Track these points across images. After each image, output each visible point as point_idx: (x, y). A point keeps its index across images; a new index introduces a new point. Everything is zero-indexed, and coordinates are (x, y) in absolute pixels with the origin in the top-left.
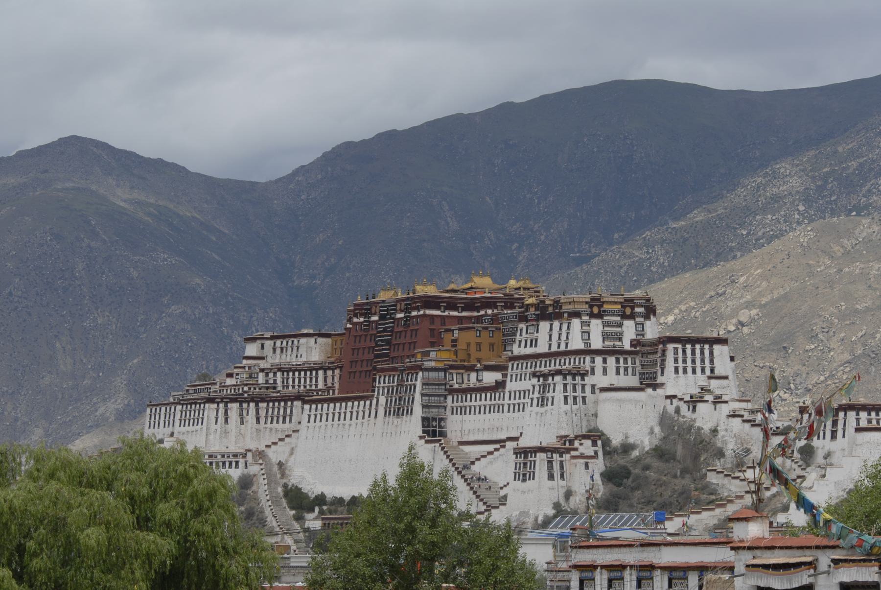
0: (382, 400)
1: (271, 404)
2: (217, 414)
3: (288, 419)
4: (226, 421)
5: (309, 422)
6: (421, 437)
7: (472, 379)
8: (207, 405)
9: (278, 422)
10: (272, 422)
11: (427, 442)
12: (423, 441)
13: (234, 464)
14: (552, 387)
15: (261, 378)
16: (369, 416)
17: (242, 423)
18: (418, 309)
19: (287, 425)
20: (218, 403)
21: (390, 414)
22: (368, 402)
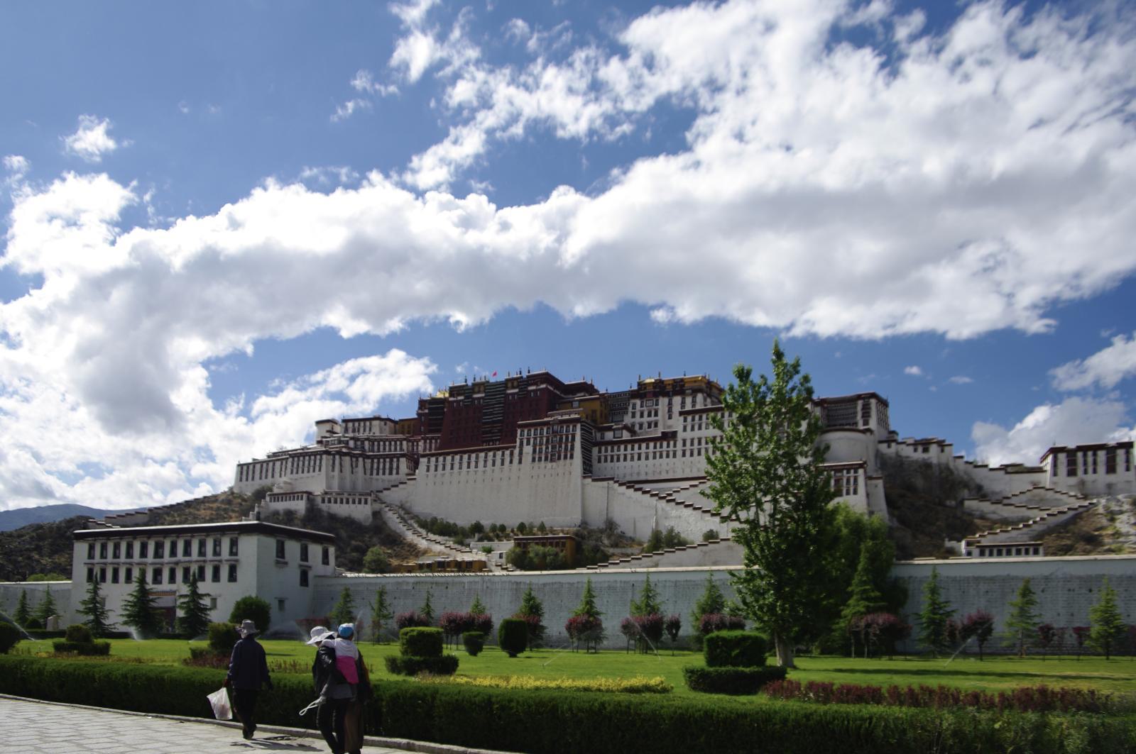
0: (528, 449)
2: (334, 463)
3: (394, 472)
5: (428, 470)
7: (609, 436)
8: (324, 456)
9: (384, 474)
10: (378, 474)
11: (594, 480)
15: (351, 444)
16: (511, 462)
17: (352, 473)
19: (394, 476)
20: (334, 455)
21: (540, 459)
22: (508, 452)
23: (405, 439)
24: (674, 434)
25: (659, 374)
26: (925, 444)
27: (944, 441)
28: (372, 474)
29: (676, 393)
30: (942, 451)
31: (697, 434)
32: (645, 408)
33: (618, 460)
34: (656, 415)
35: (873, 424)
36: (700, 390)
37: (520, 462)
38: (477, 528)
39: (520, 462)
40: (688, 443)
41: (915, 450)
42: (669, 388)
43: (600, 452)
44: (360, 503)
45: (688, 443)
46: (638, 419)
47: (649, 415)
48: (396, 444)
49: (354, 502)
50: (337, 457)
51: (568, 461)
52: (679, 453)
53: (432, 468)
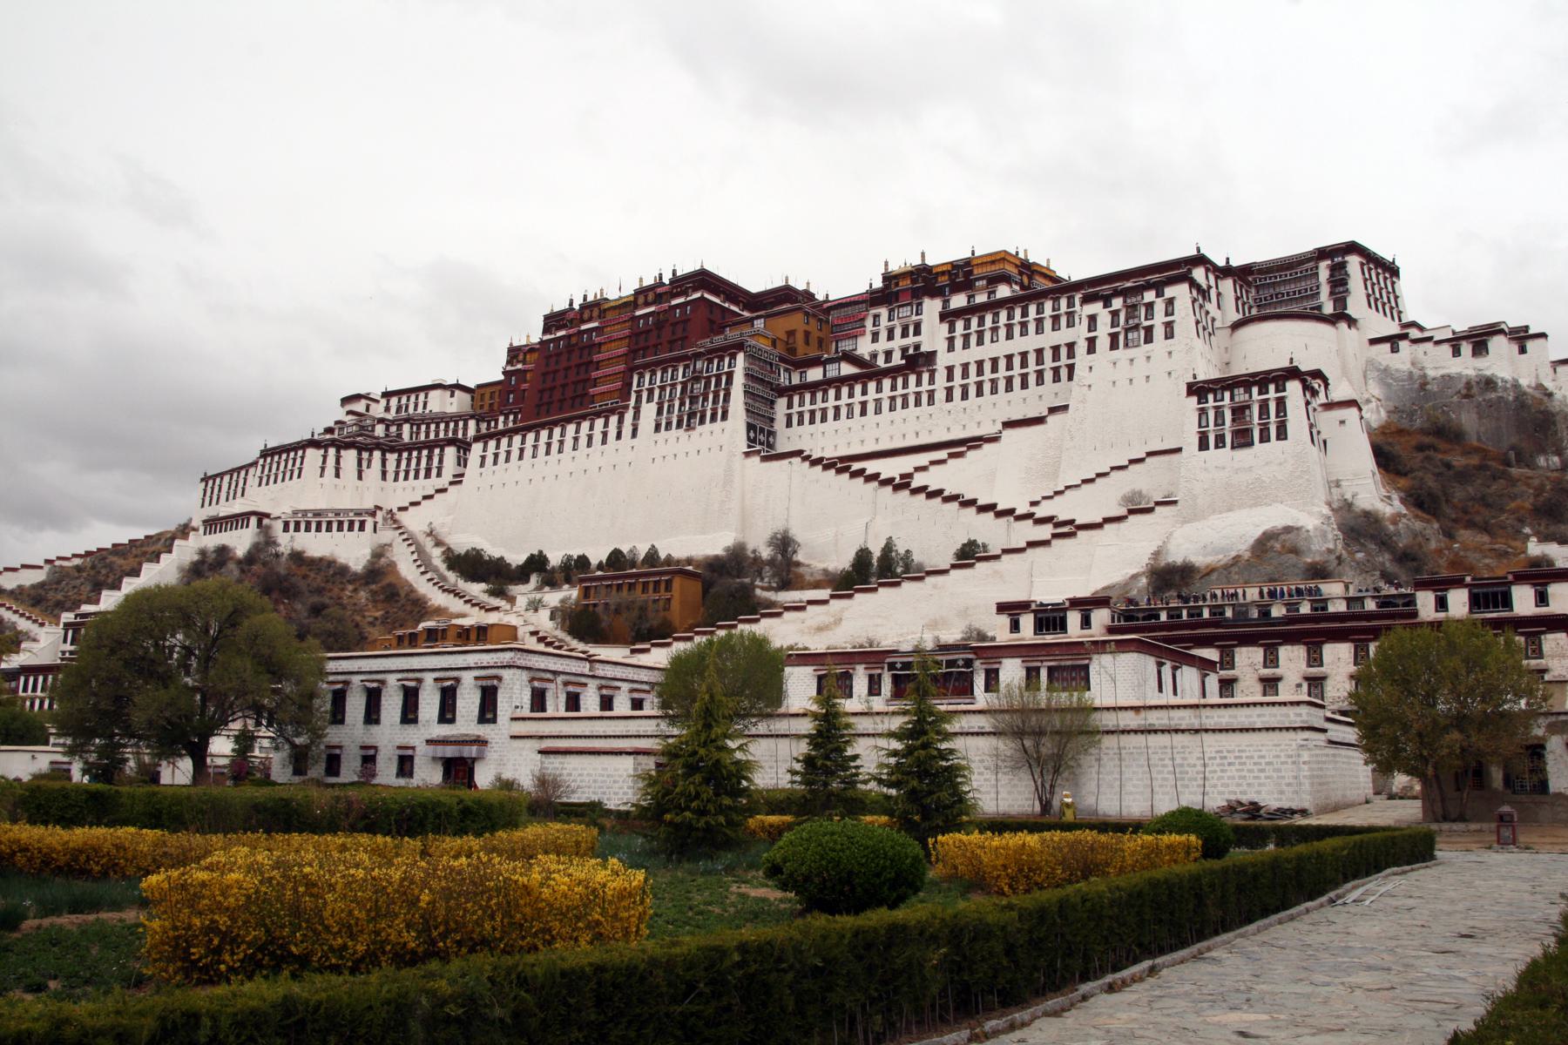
0: (649, 411)
1: (405, 455)
3: (434, 472)
4: (337, 475)
5: (482, 465)
6: (747, 454)
7: (815, 374)
8: (310, 452)
9: (416, 477)
11: (765, 459)
12: (757, 459)
13: (357, 525)
14: (1160, 306)
15: (380, 430)
16: (619, 436)
17: (360, 478)
18: (685, 293)
21: (669, 425)
22: (614, 419)
23: (472, 417)
24: (931, 357)
25: (923, 255)
26: (1479, 339)
27: (1526, 328)
28: (396, 479)
29: (956, 289)
30: (1523, 350)
31: (975, 353)
32: (896, 322)
33: (824, 419)
34: (917, 332)
35: (1356, 304)
36: (1005, 279)
37: (634, 435)
38: (537, 563)
39: (634, 435)
40: (958, 372)
41: (1456, 352)
42: (943, 280)
43: (790, 406)
44: (351, 529)
45: (958, 372)
46: (883, 344)
47: (905, 334)
48: (456, 425)
49: (340, 529)
50: (332, 451)
51: (719, 424)
52: (940, 395)
53: (489, 459)
